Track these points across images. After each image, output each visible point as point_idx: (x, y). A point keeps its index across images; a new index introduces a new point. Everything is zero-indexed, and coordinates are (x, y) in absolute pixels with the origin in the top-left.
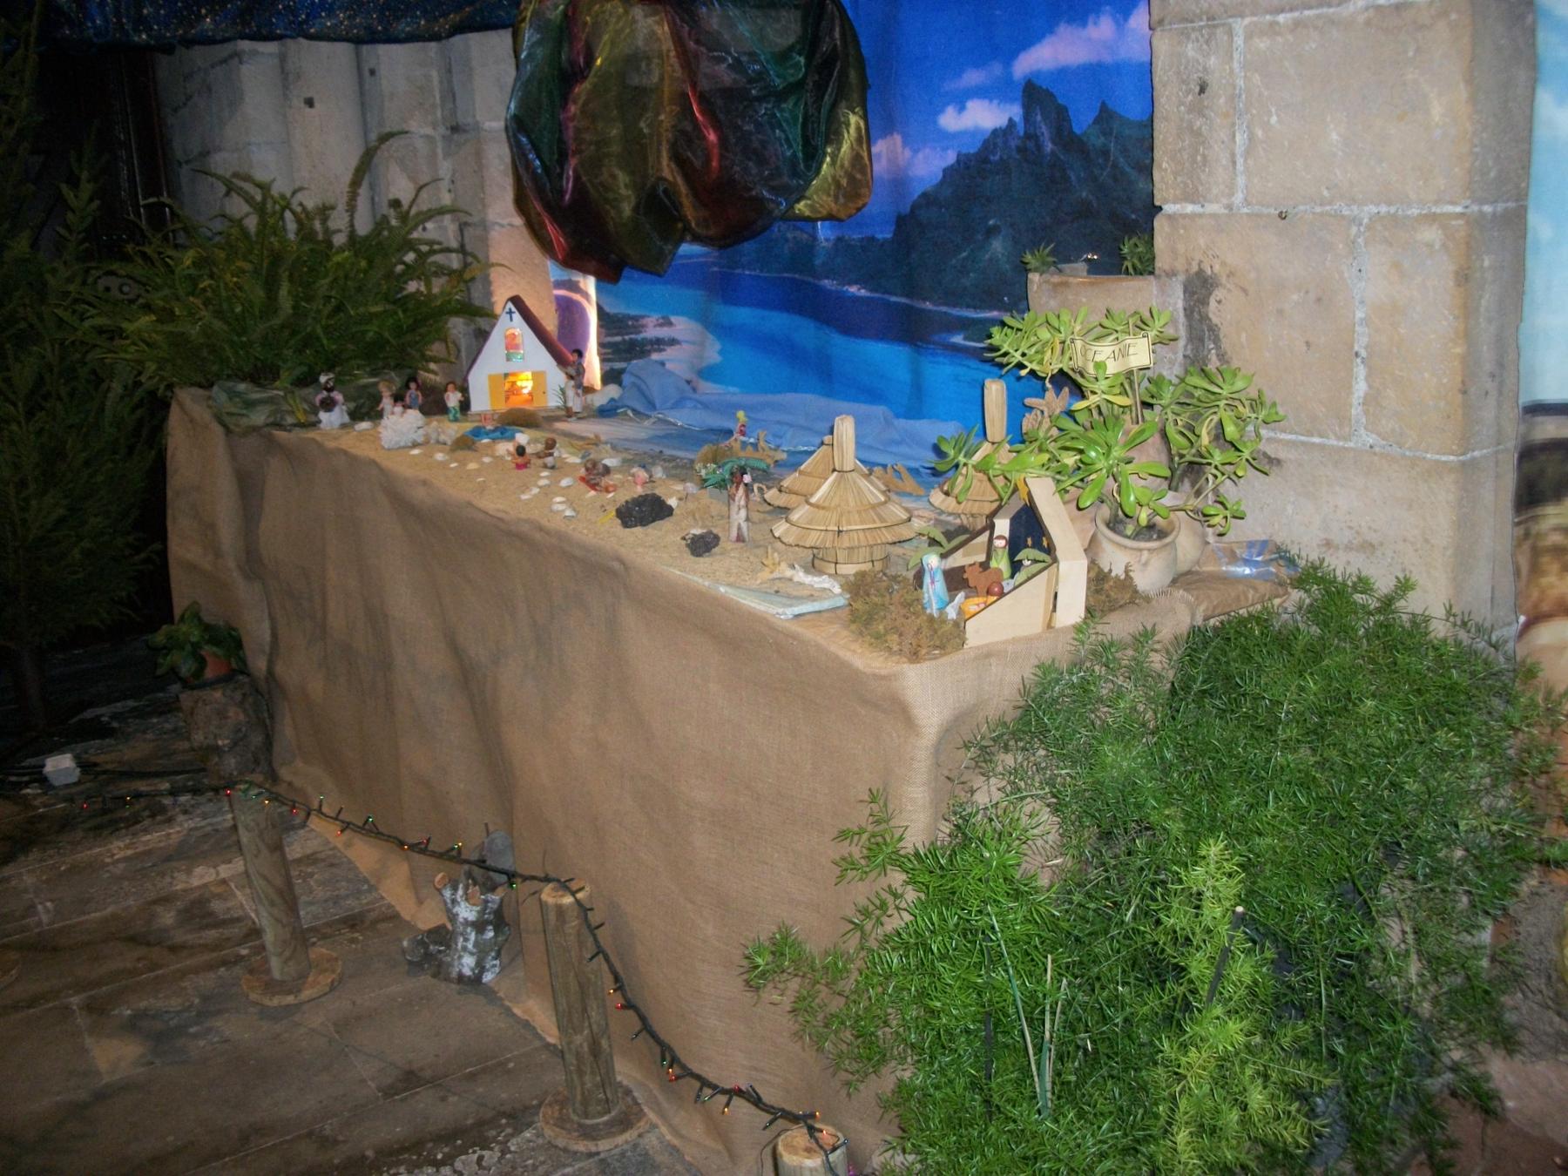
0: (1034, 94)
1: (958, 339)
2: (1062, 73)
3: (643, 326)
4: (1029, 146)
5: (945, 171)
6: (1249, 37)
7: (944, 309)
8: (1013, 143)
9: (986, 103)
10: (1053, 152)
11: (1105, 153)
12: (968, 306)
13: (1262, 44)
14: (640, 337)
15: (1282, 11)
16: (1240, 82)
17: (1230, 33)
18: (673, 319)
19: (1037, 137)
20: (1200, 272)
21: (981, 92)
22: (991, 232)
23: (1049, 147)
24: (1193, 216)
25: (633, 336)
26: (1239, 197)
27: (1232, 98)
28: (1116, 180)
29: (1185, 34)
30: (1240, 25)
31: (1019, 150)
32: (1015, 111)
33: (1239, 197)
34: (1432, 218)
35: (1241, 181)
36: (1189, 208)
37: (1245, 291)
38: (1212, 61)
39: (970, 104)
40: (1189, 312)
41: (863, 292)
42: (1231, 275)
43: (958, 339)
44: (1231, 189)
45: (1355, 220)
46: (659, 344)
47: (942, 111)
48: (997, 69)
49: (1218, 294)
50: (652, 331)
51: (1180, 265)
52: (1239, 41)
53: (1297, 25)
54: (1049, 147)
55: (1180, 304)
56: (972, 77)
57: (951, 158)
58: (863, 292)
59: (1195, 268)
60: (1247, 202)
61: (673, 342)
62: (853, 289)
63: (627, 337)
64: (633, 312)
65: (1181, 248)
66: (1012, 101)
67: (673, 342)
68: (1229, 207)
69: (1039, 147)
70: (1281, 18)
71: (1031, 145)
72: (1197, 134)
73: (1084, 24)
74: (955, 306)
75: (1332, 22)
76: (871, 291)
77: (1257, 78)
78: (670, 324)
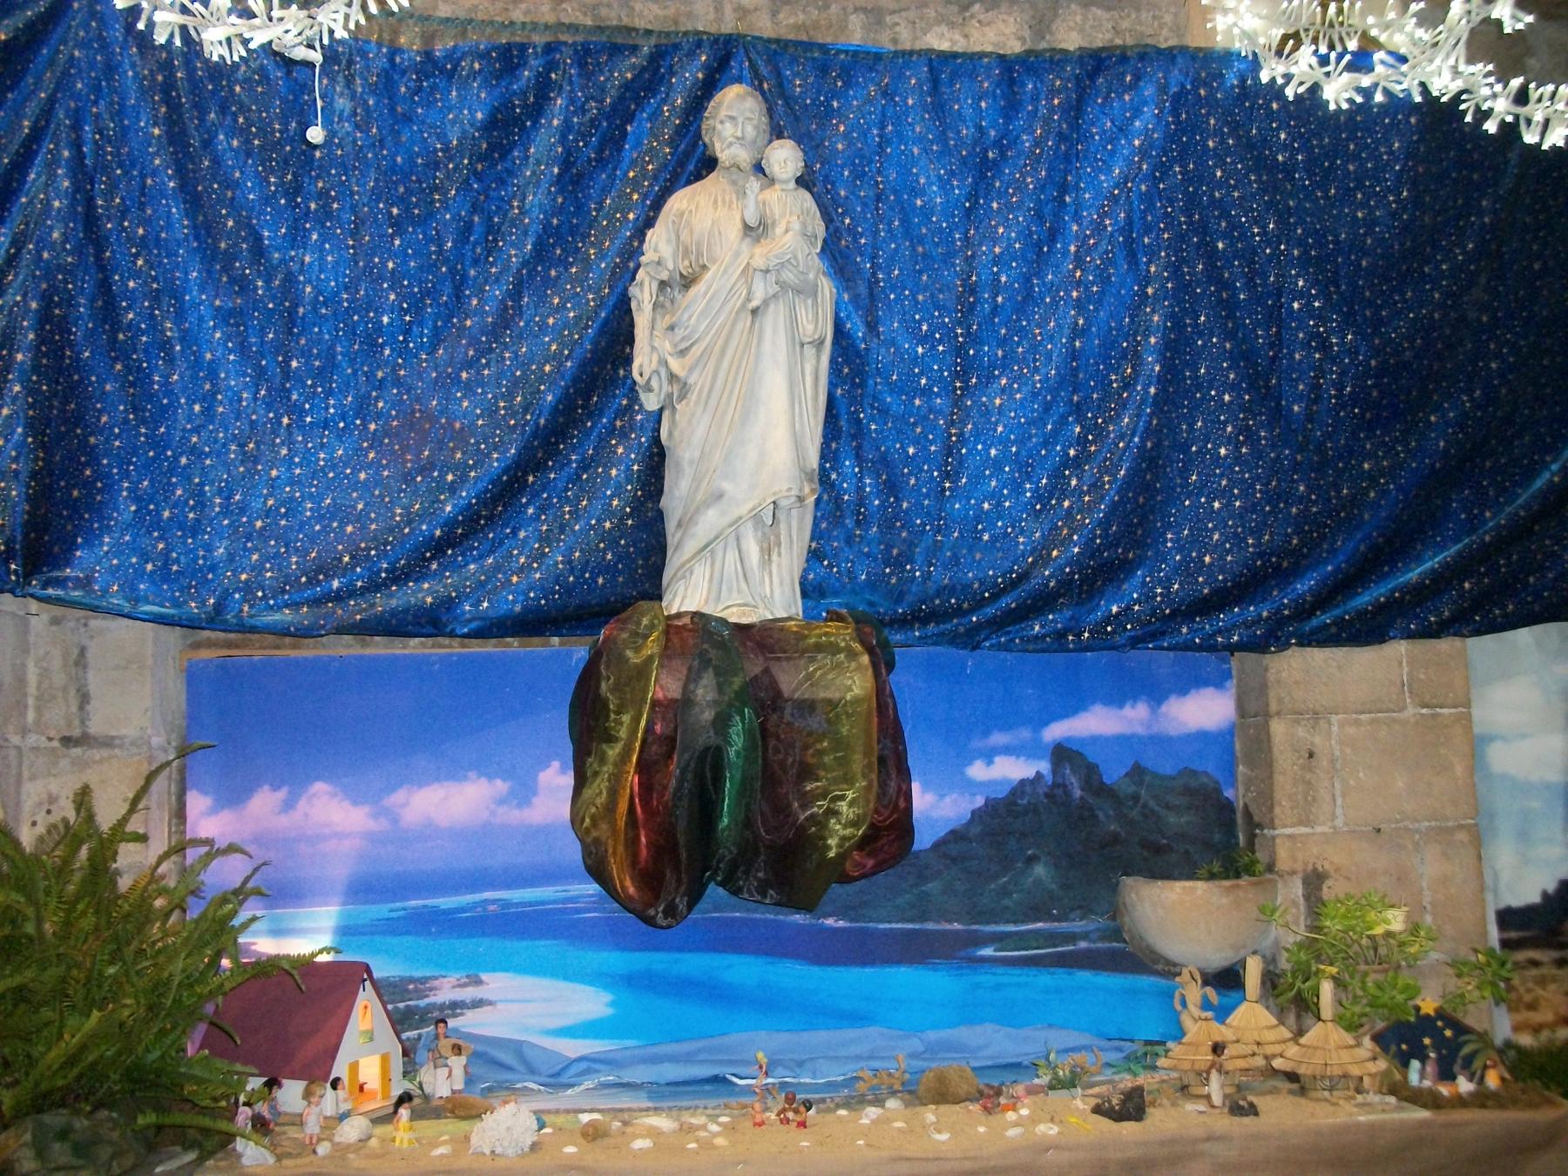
0: (1062, 754)
1: (988, 952)
2: (1095, 740)
3: (435, 989)
4: (1056, 793)
5: (973, 812)
6: (1342, 725)
7: (975, 927)
8: (1041, 790)
9: (1013, 758)
10: (1082, 798)
11: (1136, 798)
12: (1008, 922)
13: (1351, 730)
14: (422, 1003)
15: (1363, 712)
16: (1337, 753)
17: (1330, 723)
18: (484, 977)
19: (1065, 786)
20: (1315, 870)
21: (1008, 750)
22: (1031, 860)
23: (1077, 793)
24: (1308, 835)
25: (411, 1003)
26: (1339, 822)
27: (1332, 762)
28: (1145, 816)
29: (1297, 722)
30: (1334, 718)
31: (1047, 795)
32: (1044, 766)
33: (1339, 822)
34: (1461, 827)
35: (1339, 811)
36: (1303, 830)
37: (1348, 879)
38: (1317, 740)
39: (997, 759)
40: (1307, 897)
41: (841, 923)
42: (1337, 870)
43: (988, 952)
44: (1334, 817)
45: (1417, 831)
46: (456, 1007)
47: (970, 763)
48: (1025, 734)
49: (1329, 883)
50: (445, 993)
51: (1299, 867)
52: (1335, 729)
53: (1373, 721)
54: (1077, 793)
55: (1300, 892)
56: (998, 738)
57: (979, 801)
58: (841, 923)
59: (1310, 867)
60: (1346, 824)
61: (478, 1004)
62: (830, 922)
63: (401, 1005)
64: (417, 974)
65: (1300, 856)
66: (1040, 758)
67: (478, 1004)
68: (1334, 827)
69: (1067, 793)
70: (1363, 717)
71: (1059, 792)
72: (1309, 783)
73: (1121, 706)
74: (988, 923)
75: (1394, 720)
76: (852, 920)
77: (1348, 751)
78: (479, 982)
